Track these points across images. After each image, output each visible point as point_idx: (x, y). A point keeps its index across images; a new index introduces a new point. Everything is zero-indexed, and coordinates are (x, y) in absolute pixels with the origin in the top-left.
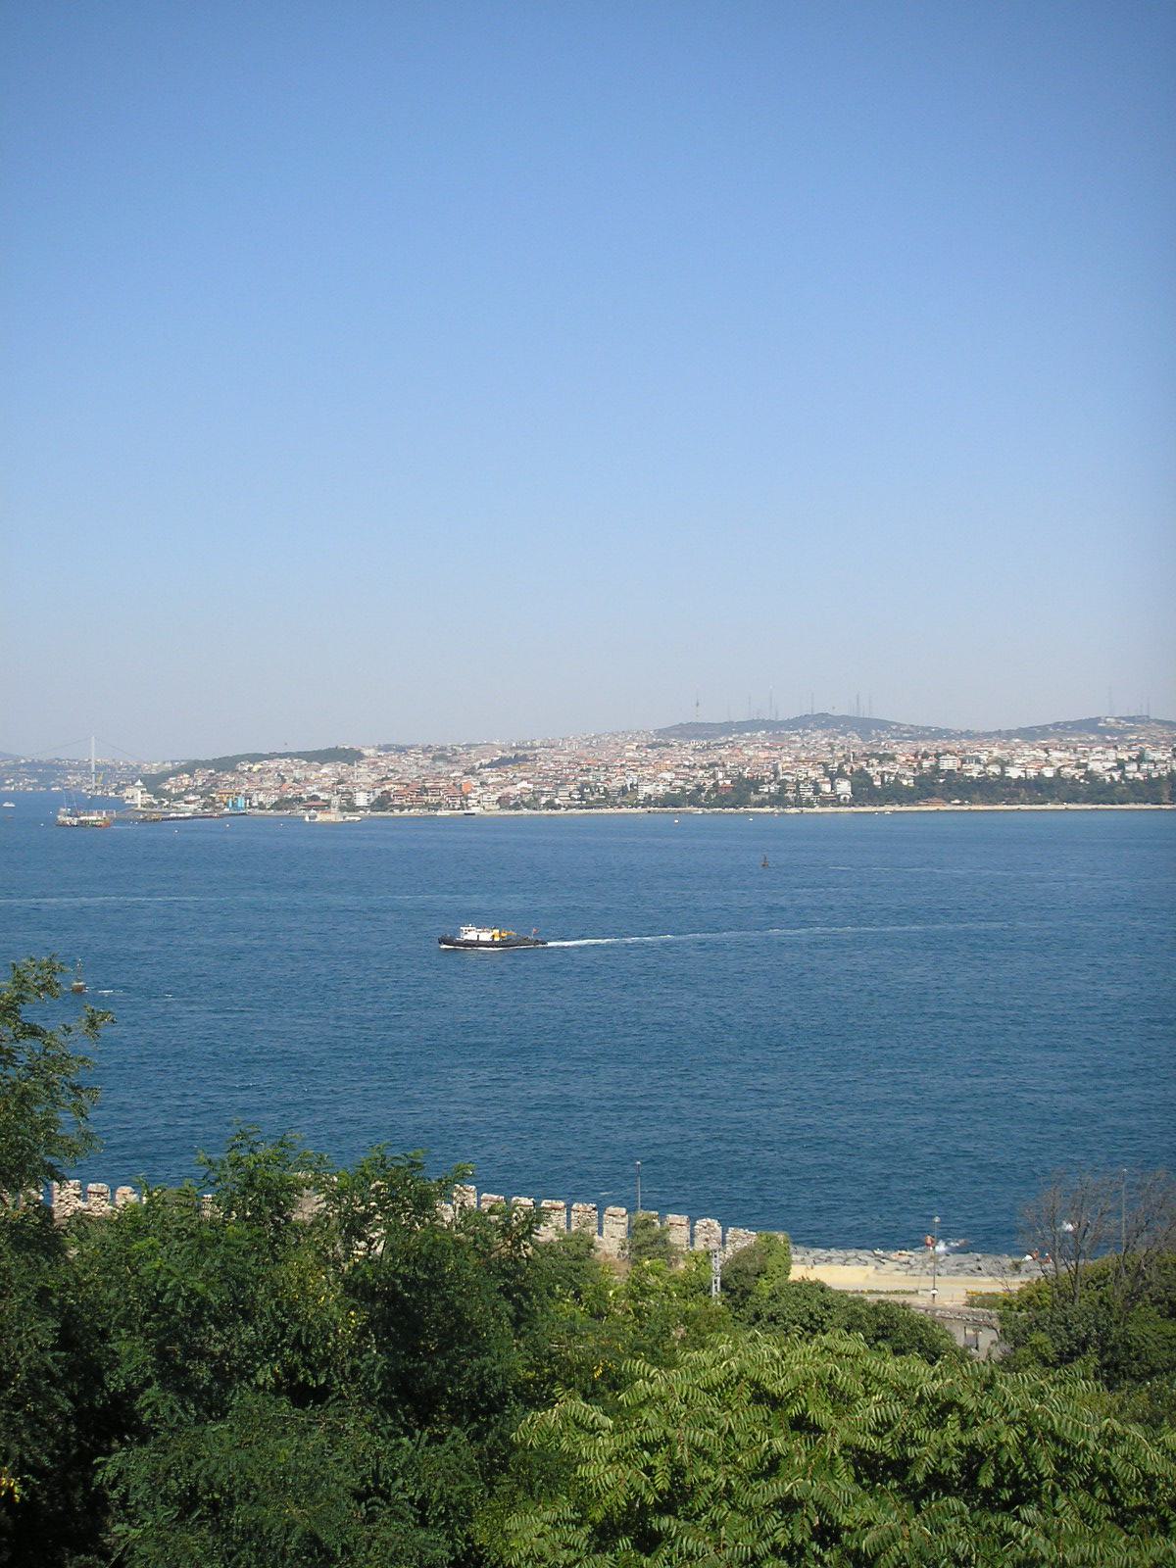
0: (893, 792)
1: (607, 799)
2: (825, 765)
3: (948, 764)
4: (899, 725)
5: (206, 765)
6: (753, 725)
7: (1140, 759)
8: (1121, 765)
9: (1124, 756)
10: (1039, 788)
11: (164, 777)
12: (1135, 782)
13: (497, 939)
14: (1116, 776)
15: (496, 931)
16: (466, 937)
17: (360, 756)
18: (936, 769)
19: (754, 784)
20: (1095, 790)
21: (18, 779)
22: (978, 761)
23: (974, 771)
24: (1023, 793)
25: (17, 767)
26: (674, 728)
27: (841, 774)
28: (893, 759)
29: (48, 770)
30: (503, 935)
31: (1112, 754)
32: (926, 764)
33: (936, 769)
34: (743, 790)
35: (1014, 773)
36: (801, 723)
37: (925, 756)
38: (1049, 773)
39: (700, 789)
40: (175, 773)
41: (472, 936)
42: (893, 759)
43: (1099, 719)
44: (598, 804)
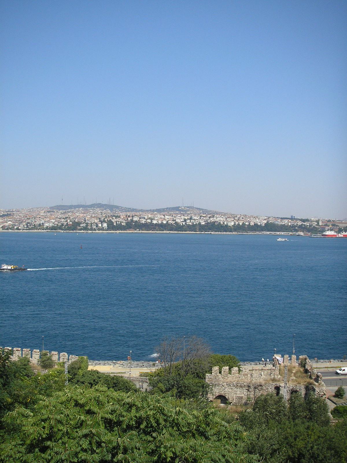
0: (119, 227)
1: (35, 227)
2: (100, 218)
3: (136, 219)
4: (122, 207)
6: (79, 206)
7: (191, 219)
8: (185, 220)
9: (186, 218)
10: (162, 226)
13: (13, 268)
14: (184, 223)
15: (12, 266)
16: (4, 268)
18: (132, 220)
19: (79, 224)
20: (178, 227)
22: (144, 218)
23: (143, 221)
27: (104, 221)
28: (119, 217)
30: (14, 267)
31: (183, 217)
32: (129, 219)
33: (132, 220)
34: (75, 225)
35: (155, 222)
36: (92, 206)
37: (129, 216)
38: (165, 222)
39: (62, 225)
41: (5, 267)
42: (119, 217)
43: (179, 207)
44: (32, 229)
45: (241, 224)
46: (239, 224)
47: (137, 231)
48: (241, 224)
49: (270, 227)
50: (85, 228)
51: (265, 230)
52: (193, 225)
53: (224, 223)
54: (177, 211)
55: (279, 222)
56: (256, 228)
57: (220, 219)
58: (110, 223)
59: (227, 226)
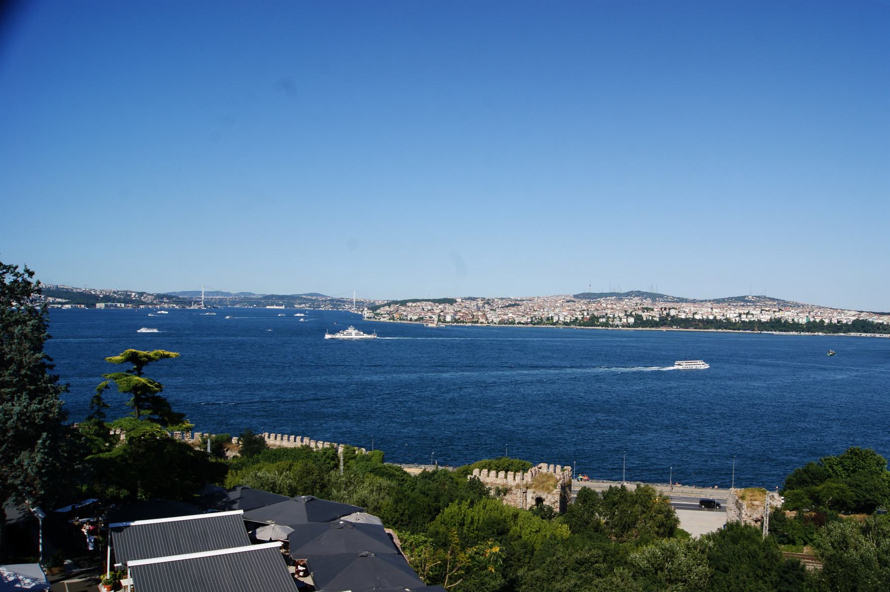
0: (651, 323)
1: (541, 322)
2: (626, 311)
3: (673, 313)
5: (396, 302)
7: (748, 314)
8: (740, 315)
9: (742, 312)
10: (707, 323)
11: (379, 307)
12: (744, 322)
14: (737, 319)
18: (668, 315)
19: (598, 318)
20: (728, 324)
23: (683, 316)
24: (701, 325)
25: (325, 301)
27: (631, 315)
28: (653, 310)
31: (737, 311)
32: (665, 312)
33: (668, 315)
34: (593, 320)
35: (697, 317)
37: (665, 309)
38: (711, 317)
39: (577, 319)
40: (384, 306)
42: (653, 310)
44: (538, 323)
45: (818, 320)
46: (814, 321)
47: (675, 328)
48: (818, 320)
49: (861, 325)
50: (606, 324)
52: (750, 322)
56: (839, 327)
57: (788, 315)
58: (638, 318)
59: (798, 324)
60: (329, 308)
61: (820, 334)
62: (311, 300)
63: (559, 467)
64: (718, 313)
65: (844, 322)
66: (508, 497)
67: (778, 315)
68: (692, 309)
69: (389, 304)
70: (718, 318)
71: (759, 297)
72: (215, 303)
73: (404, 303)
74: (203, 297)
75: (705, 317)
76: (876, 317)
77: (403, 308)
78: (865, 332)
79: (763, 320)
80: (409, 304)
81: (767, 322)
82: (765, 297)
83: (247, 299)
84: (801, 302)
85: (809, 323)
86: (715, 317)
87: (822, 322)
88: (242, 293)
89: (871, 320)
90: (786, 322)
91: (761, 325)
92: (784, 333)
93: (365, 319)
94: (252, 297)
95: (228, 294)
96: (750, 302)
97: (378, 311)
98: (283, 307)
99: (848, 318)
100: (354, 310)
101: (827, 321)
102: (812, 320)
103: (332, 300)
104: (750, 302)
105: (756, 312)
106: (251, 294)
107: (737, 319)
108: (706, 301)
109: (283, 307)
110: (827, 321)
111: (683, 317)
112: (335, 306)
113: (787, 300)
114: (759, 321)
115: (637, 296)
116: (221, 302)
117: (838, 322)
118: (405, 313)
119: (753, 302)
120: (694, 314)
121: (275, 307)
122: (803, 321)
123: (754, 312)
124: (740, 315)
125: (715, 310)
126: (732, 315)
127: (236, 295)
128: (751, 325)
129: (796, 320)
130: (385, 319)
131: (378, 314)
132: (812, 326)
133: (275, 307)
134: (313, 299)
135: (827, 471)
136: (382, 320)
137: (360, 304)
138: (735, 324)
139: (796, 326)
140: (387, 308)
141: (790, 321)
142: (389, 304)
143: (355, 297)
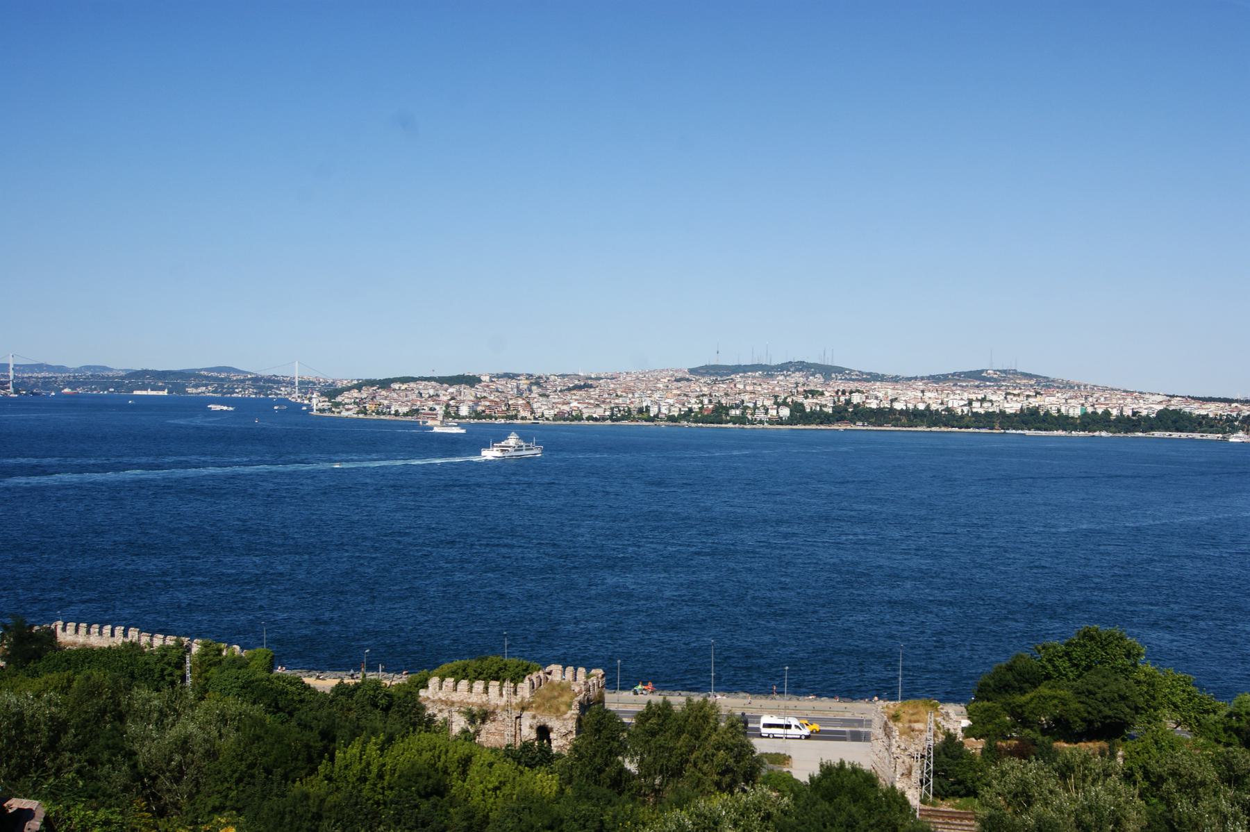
0: (819, 417)
2: (776, 397)
3: (856, 398)
4: (851, 371)
5: (371, 383)
6: (754, 368)
7: (983, 400)
8: (970, 403)
9: (973, 397)
10: (914, 416)
12: (976, 414)
14: (966, 409)
17: (479, 381)
18: (848, 402)
19: (727, 409)
20: (950, 418)
21: (244, 389)
22: (877, 398)
23: (873, 405)
24: (904, 420)
25: (243, 381)
26: (701, 368)
27: (785, 404)
28: (822, 394)
29: (264, 383)
31: (966, 396)
32: (842, 399)
33: (848, 402)
34: (720, 413)
35: (898, 406)
36: (785, 368)
37: (844, 393)
38: (921, 407)
39: (691, 410)
42: (822, 394)
43: (982, 371)
45: (1100, 411)
46: (1095, 413)
47: (859, 426)
48: (1100, 411)
49: (1171, 419)
50: (741, 420)
51: (1158, 429)
52: (988, 414)
53: (1059, 411)
54: (977, 379)
55: (1198, 410)
57: (1051, 403)
58: (797, 408)
59: (1067, 417)
60: (250, 393)
61: (1104, 434)
62: (216, 379)
63: (582, 670)
64: (933, 400)
65: (1144, 413)
66: (489, 726)
67: (1034, 402)
68: (890, 392)
69: (359, 387)
70: (934, 407)
71: (1004, 372)
72: (35, 385)
73: (385, 384)
74: (11, 374)
75: (911, 406)
76: (1197, 405)
77: (384, 393)
78: (1178, 430)
79: (1009, 411)
80: (396, 386)
81: (1015, 415)
82: (1015, 372)
83: (98, 377)
84: (1074, 379)
85: (1085, 415)
86: (928, 406)
87: (1107, 413)
88: (88, 368)
89: (1187, 410)
90: (1047, 413)
91: (1005, 419)
92: (1043, 433)
93: (314, 412)
94: (106, 373)
95: (61, 369)
96: (989, 380)
97: (339, 399)
98: (165, 393)
99: (1150, 407)
100: (296, 397)
101: (1115, 412)
102: (1090, 410)
103: (256, 380)
104: (989, 380)
105: (998, 397)
106: (105, 368)
107: (966, 409)
108: (916, 378)
109: (165, 393)
110: (1115, 412)
111: (874, 406)
112: (261, 389)
113: (1052, 376)
114: (1002, 413)
115: (799, 370)
116: (47, 383)
117: (1134, 414)
118: (386, 402)
119: (995, 380)
120: (892, 401)
121: (150, 393)
122: (1076, 412)
123: (994, 398)
124: (970, 403)
125: (928, 394)
126: (957, 402)
127: (76, 370)
128: (988, 419)
129: (1063, 410)
130: (350, 413)
131: (337, 405)
132: (1090, 421)
133: (150, 393)
134: (222, 379)
135: (1044, 667)
136: (345, 414)
137: (307, 386)
138: (962, 417)
139: (1063, 421)
140: (355, 393)
141: (1054, 412)
142: (359, 387)
143: (297, 372)
